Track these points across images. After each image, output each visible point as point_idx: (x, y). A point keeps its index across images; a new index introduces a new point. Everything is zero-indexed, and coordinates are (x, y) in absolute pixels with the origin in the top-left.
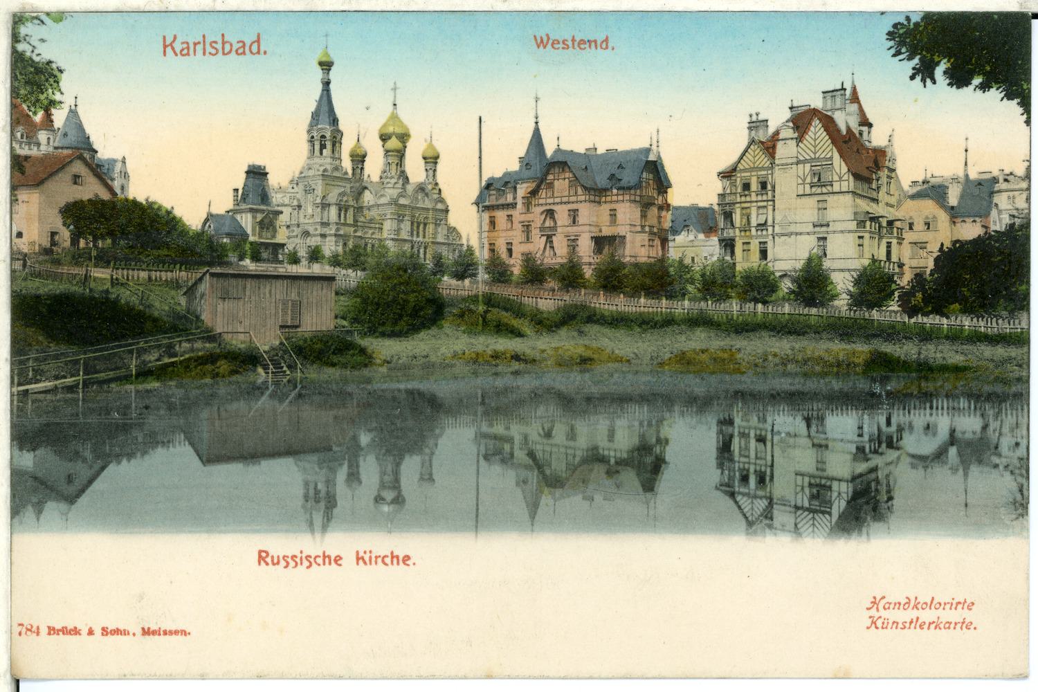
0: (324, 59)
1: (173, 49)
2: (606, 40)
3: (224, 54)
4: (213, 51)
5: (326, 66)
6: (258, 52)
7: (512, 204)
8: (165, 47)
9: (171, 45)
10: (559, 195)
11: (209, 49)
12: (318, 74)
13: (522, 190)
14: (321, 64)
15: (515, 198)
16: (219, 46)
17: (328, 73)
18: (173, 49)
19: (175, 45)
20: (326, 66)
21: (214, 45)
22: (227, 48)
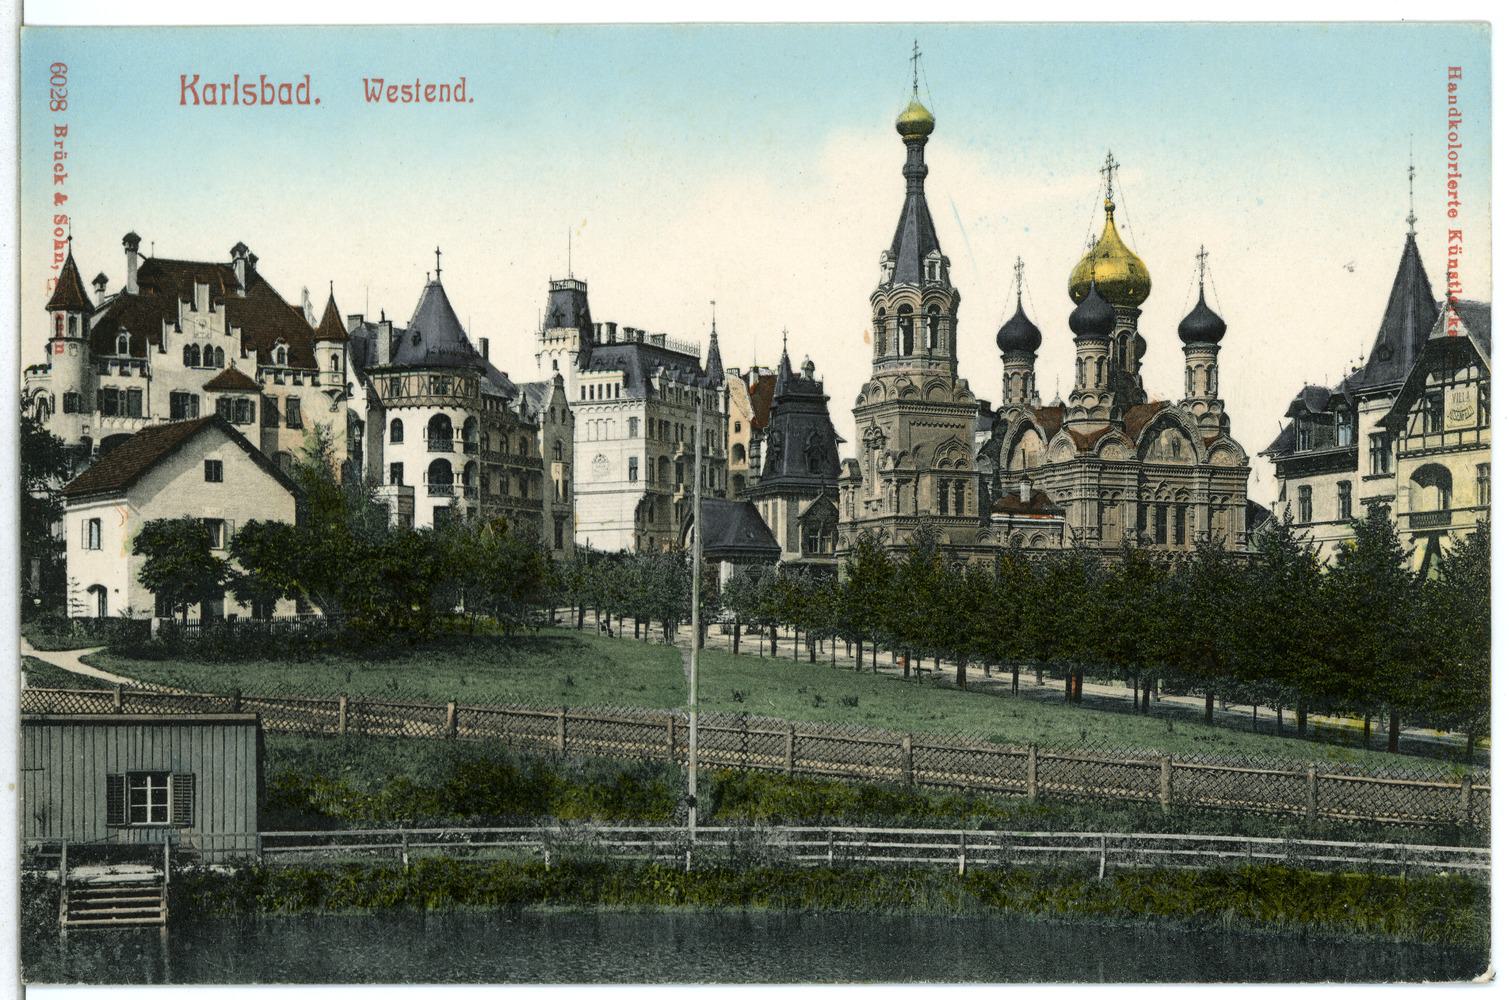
0: (914, 117)
1: (194, 91)
2: (462, 85)
3: (263, 102)
4: (250, 99)
5: (916, 133)
6: (308, 101)
7: (1344, 454)
8: (184, 89)
9: (192, 86)
10: (1458, 425)
11: (241, 96)
12: (897, 152)
13: (1369, 420)
14: (902, 128)
15: (1355, 438)
16: (257, 90)
17: (921, 150)
18: (194, 91)
19: (195, 86)
20: (916, 133)
21: (247, 89)
22: (268, 91)
